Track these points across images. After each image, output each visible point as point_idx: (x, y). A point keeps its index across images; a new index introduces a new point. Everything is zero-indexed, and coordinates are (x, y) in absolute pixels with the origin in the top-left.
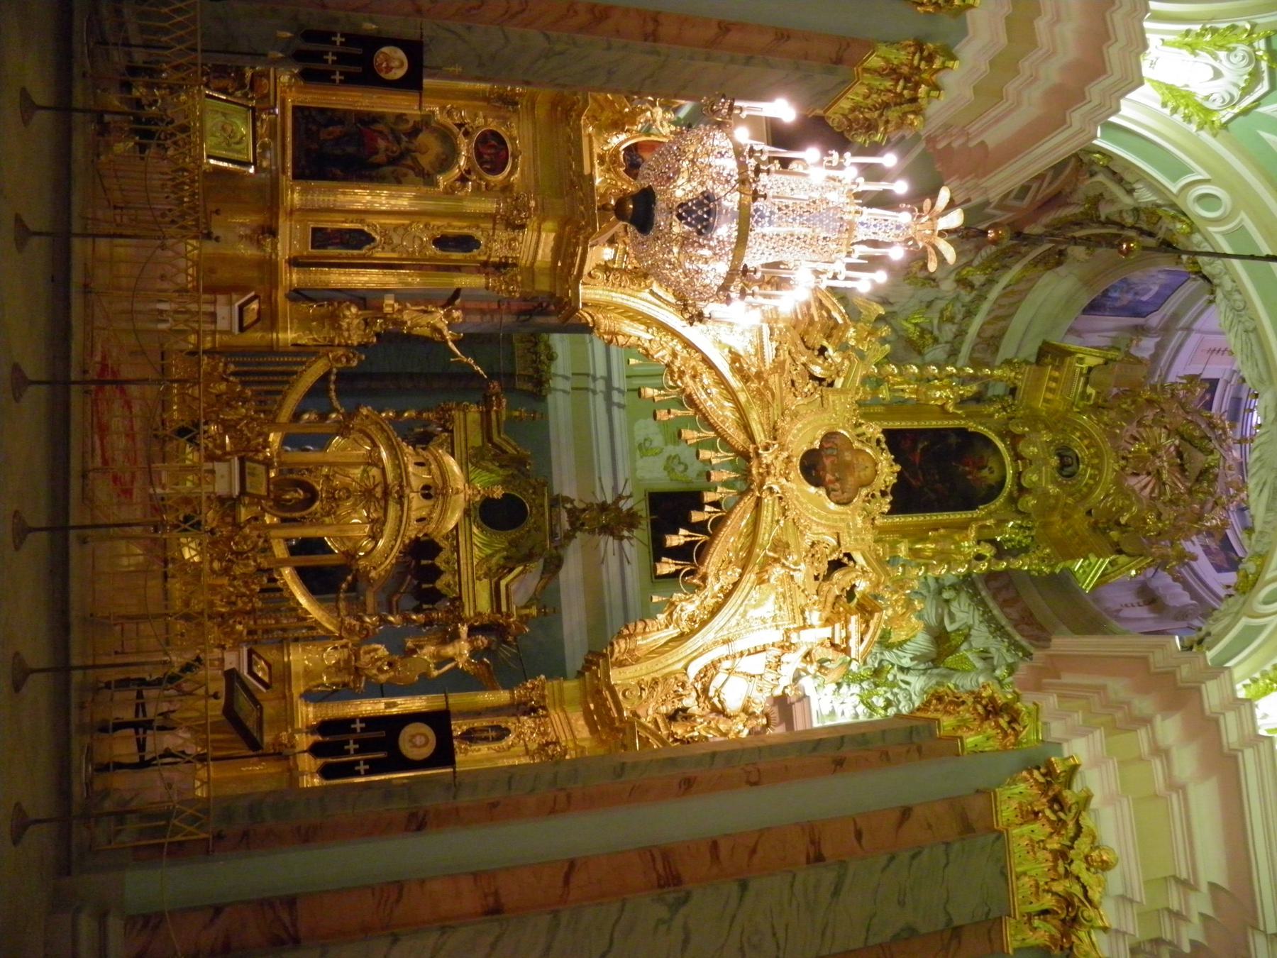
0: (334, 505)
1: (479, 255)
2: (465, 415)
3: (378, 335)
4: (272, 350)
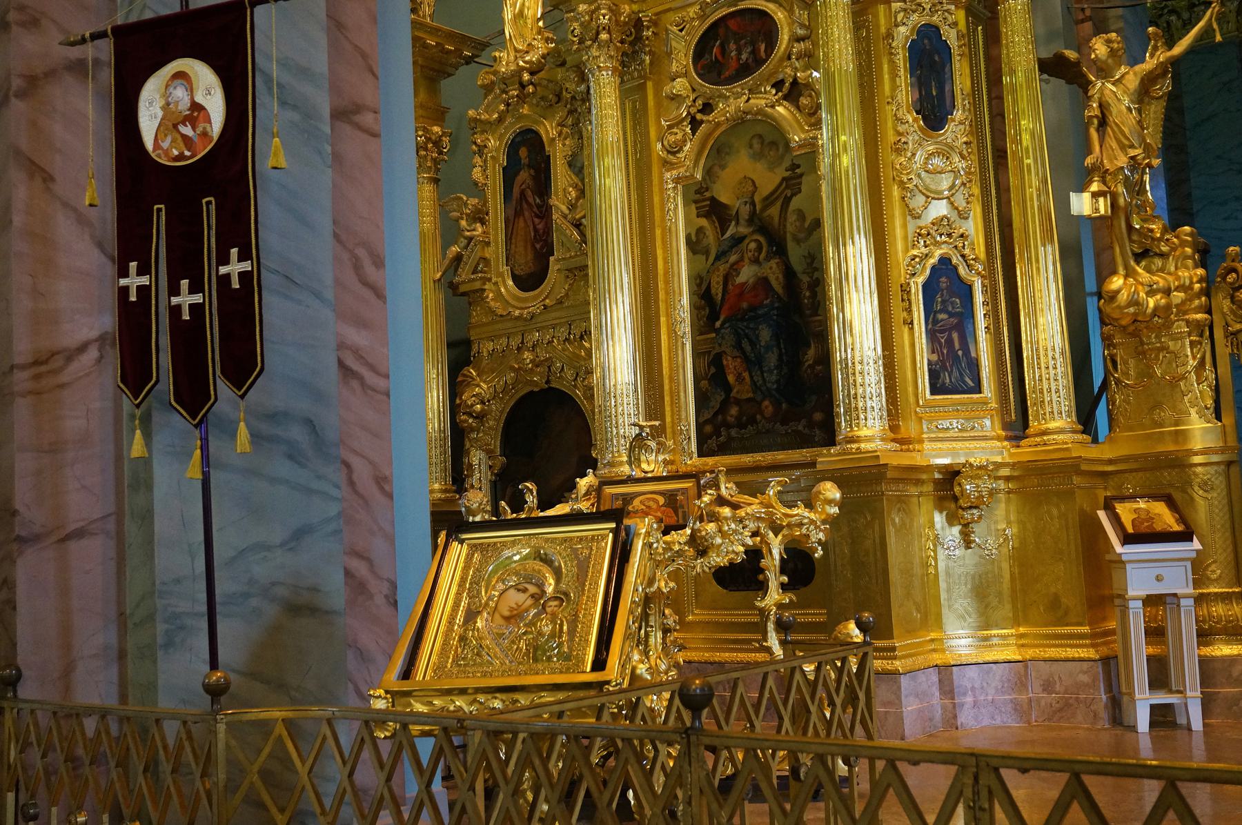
3: (1174, 226)
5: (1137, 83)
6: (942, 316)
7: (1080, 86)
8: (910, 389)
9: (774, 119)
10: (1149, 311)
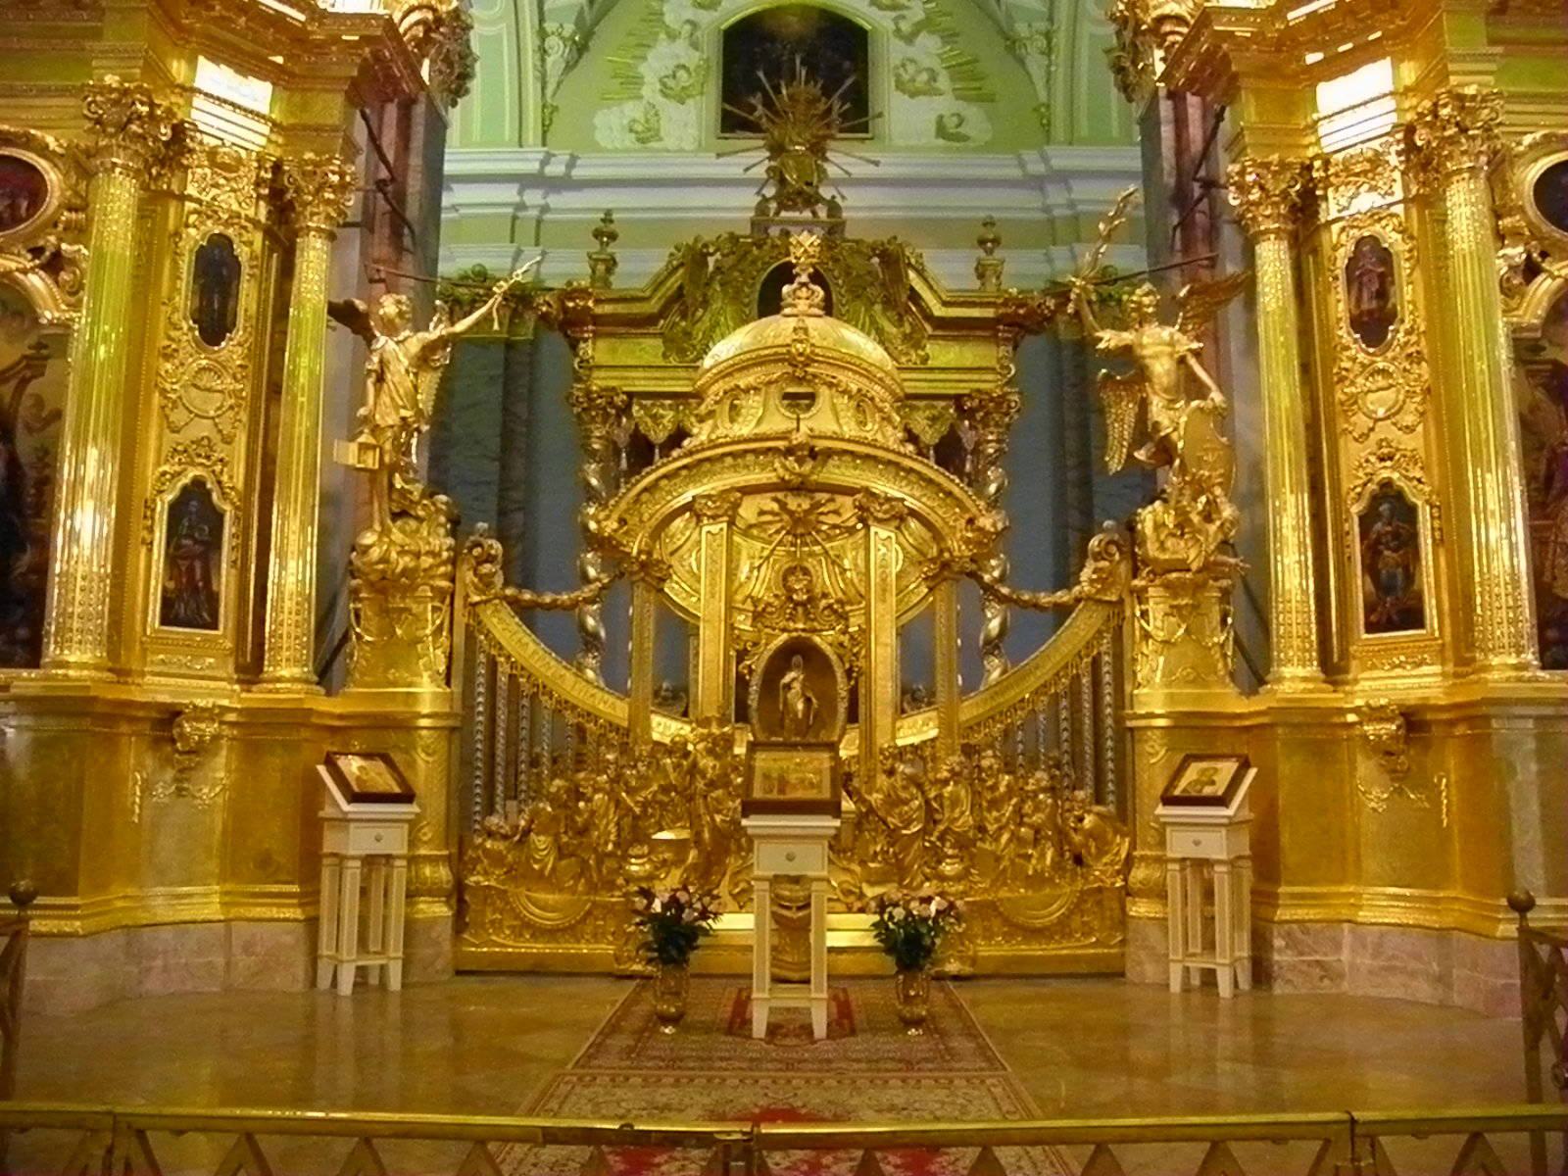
0: (824, 603)
1: (249, 247)
2: (599, 367)
4: (456, 730)
6: (187, 542)
7: (365, 338)
8: (139, 617)
9: (25, 288)
10: (398, 570)
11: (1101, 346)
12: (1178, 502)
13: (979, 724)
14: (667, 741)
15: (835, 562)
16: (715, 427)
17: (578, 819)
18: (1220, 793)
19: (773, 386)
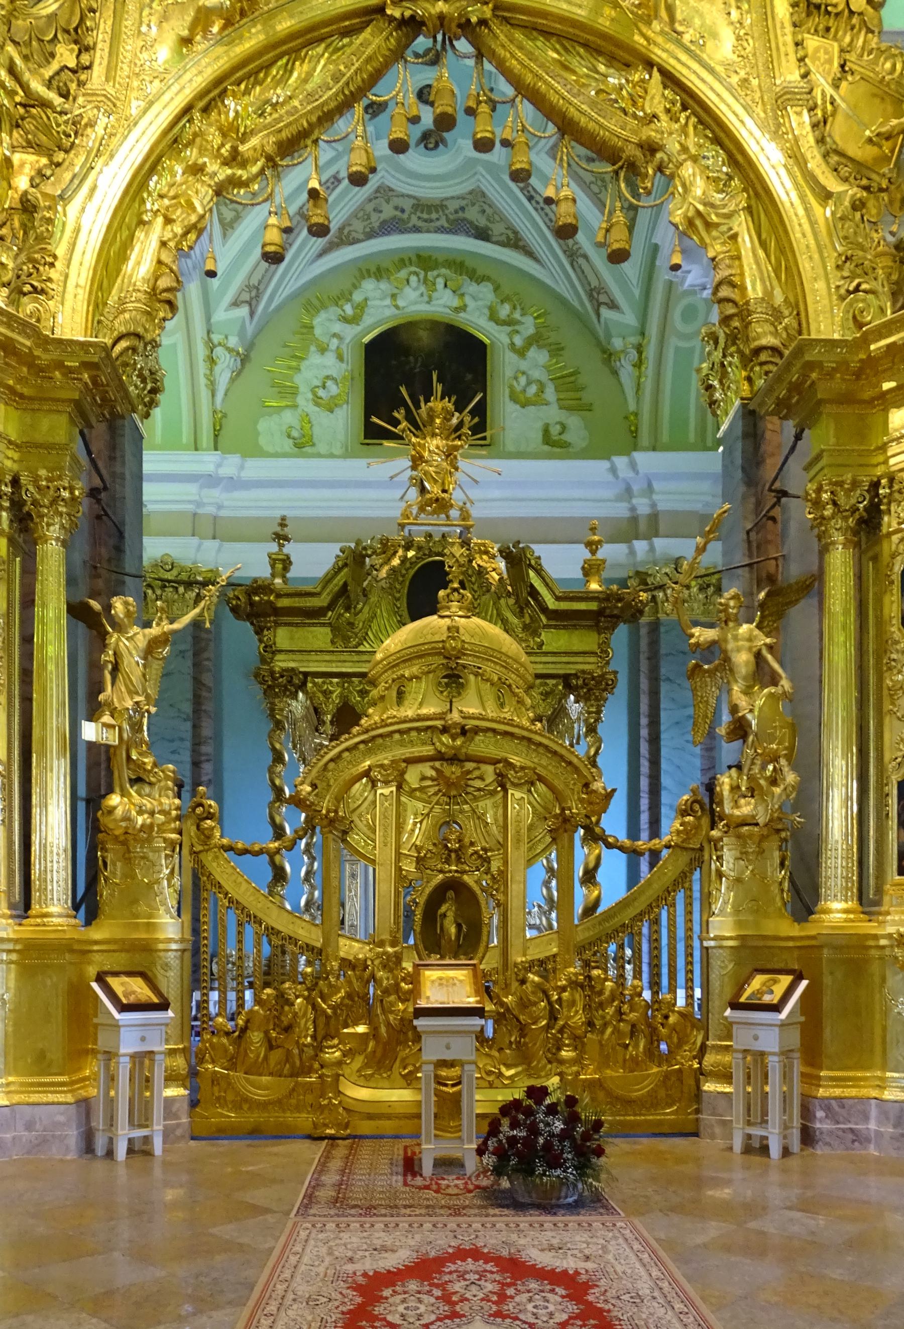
0: (471, 851)
5: (146, 643)
7: (99, 633)
10: (138, 826)
11: (693, 641)
12: (750, 770)
13: (590, 944)
14: (351, 958)
15: (481, 818)
16: (385, 709)
17: (283, 1018)
18: (775, 1002)
19: (431, 675)
